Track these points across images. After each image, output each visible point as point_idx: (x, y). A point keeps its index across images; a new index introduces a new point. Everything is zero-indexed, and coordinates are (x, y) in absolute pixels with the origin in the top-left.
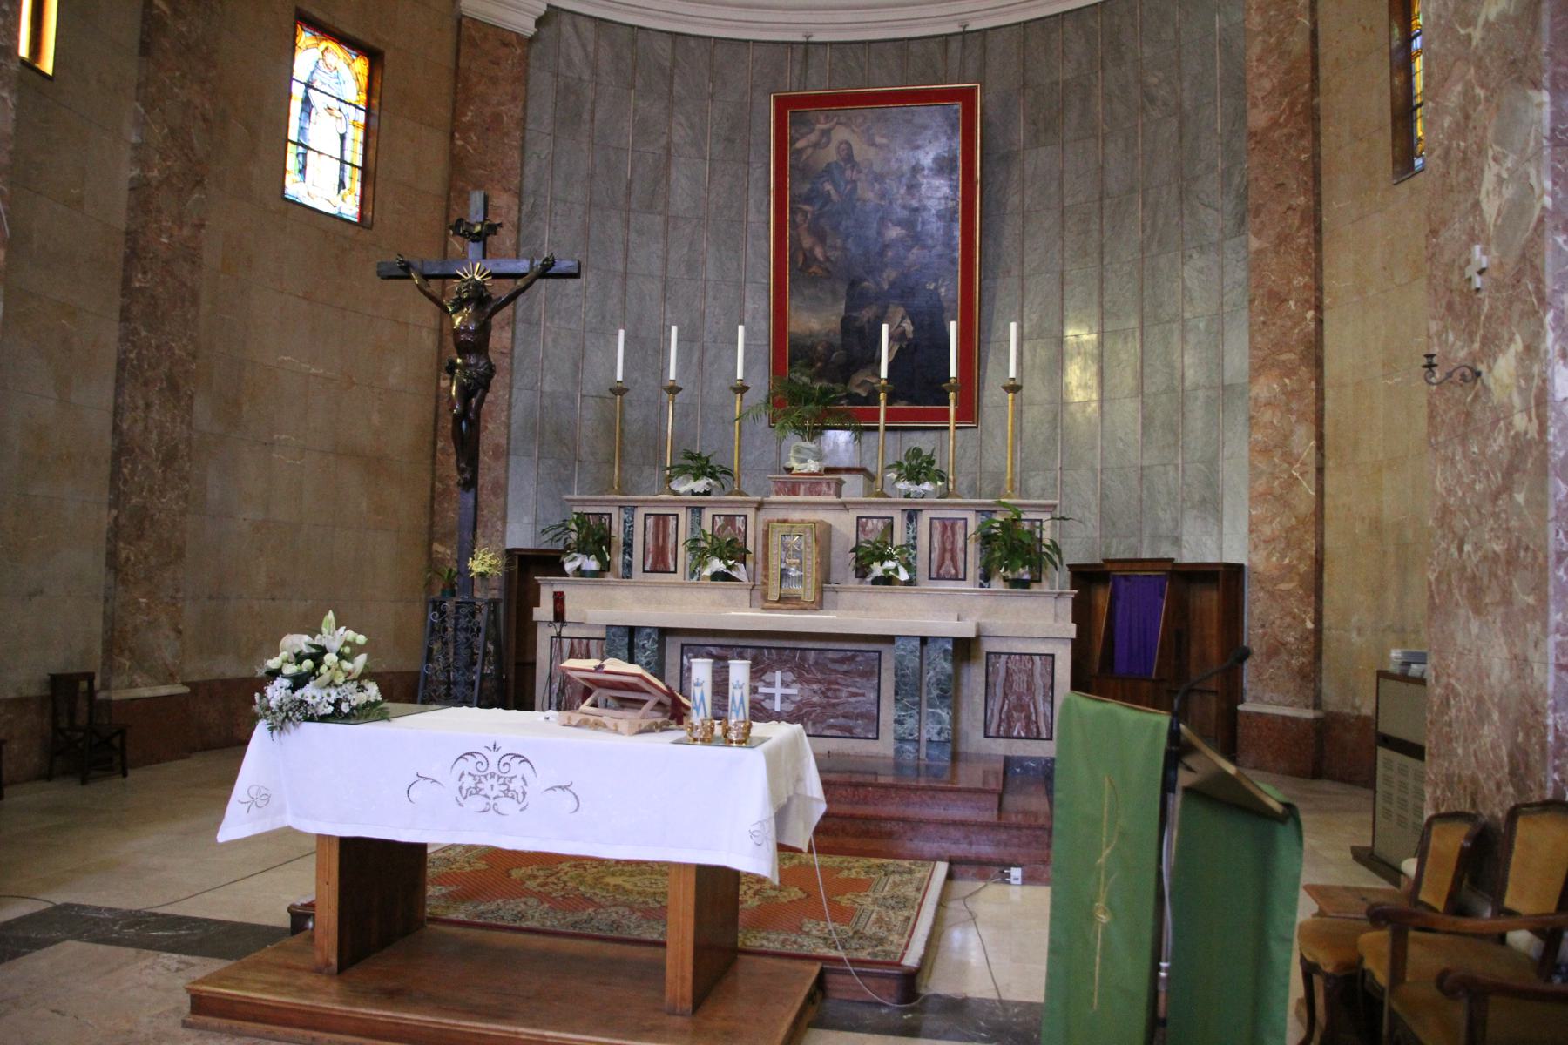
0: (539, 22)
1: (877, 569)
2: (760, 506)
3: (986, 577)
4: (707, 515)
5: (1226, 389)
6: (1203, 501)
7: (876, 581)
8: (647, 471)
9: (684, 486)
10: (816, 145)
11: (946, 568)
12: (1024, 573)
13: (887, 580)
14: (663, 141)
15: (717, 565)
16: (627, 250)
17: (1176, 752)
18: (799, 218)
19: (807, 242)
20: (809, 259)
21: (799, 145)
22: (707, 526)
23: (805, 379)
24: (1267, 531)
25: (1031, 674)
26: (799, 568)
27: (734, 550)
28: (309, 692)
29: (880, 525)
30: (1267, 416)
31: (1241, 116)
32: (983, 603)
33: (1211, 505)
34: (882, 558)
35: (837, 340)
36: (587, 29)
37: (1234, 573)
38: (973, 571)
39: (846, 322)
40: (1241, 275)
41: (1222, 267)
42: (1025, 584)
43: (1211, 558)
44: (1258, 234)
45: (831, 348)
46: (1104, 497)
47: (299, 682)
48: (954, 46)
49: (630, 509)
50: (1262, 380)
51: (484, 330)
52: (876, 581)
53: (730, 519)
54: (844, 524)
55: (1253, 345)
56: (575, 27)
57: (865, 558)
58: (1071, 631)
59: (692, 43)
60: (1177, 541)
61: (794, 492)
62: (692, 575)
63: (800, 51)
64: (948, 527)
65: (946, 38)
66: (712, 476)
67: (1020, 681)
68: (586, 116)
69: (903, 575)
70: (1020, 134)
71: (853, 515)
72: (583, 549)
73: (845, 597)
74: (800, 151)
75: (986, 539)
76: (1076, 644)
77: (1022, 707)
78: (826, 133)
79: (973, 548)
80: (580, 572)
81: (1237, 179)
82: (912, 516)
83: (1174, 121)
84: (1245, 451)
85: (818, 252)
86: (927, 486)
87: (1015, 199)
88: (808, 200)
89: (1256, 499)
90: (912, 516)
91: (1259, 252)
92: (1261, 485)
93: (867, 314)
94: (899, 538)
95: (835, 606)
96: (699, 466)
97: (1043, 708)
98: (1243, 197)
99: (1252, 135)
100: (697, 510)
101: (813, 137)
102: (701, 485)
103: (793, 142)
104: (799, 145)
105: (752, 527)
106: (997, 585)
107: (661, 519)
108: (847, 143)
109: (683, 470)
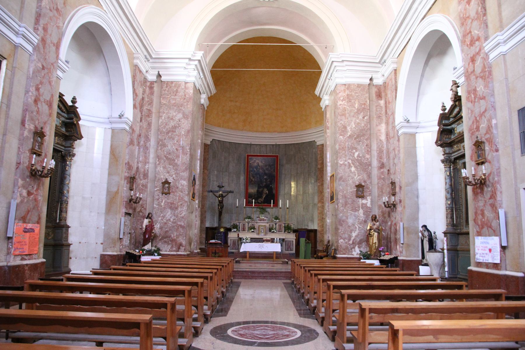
0: (211, 142)
1: (272, 231)
2: (257, 223)
3: (285, 232)
4: (250, 224)
5: (315, 204)
6: (311, 220)
7: (272, 232)
8: (226, 214)
9: (247, 220)
10: (253, 163)
11: (280, 231)
12: (290, 231)
13: (273, 232)
14: (228, 160)
15: (253, 230)
16: (223, 178)
17: (306, 240)
18: (250, 174)
19: (252, 178)
20: (252, 181)
21: (250, 162)
22: (250, 225)
23: (251, 200)
24: (320, 225)
25: (291, 243)
26: (263, 230)
27: (254, 228)
28: (247, 241)
29: (272, 225)
30: (320, 209)
31: (317, 165)
32: (285, 235)
33: (312, 221)
34: (273, 230)
35: (256, 194)
36: (217, 141)
37: (316, 230)
38: (283, 231)
39: (258, 191)
40: (317, 188)
41: (314, 187)
42: (290, 232)
43: (313, 228)
44: (319, 183)
45: (255, 195)
46: (297, 219)
47: (246, 240)
48: (274, 146)
49: (240, 223)
50: (319, 203)
51: (222, 200)
52: (272, 232)
53: (253, 224)
54: (267, 225)
55: (318, 198)
56: (215, 142)
57: (270, 230)
58: (295, 238)
59: (233, 144)
60: (308, 226)
61: (261, 221)
62: (248, 231)
63: (250, 146)
64: (280, 225)
65: (273, 145)
66: (251, 219)
67: (289, 244)
68: (217, 156)
69: (275, 231)
70: (285, 162)
71: (269, 224)
72: (234, 228)
73: (268, 234)
74: (251, 163)
75: (285, 227)
76: (296, 240)
77: (290, 247)
78: (255, 161)
79: (283, 228)
80: (234, 231)
81: (316, 174)
82: (276, 224)
83: (308, 164)
84: (317, 214)
85: (253, 180)
86: (278, 221)
87: (284, 172)
88: (252, 171)
89: (319, 220)
90: (276, 224)
91: (319, 186)
92: (319, 218)
93: (261, 190)
94: (274, 227)
95: (267, 235)
96: (249, 218)
97: (292, 247)
98: (317, 177)
99: (318, 168)
100: (248, 223)
101: (253, 161)
102: (249, 220)
103: (250, 162)
104: (250, 162)
105: (256, 226)
106: (286, 232)
107: (244, 224)
108: (258, 163)
109: (247, 218)
